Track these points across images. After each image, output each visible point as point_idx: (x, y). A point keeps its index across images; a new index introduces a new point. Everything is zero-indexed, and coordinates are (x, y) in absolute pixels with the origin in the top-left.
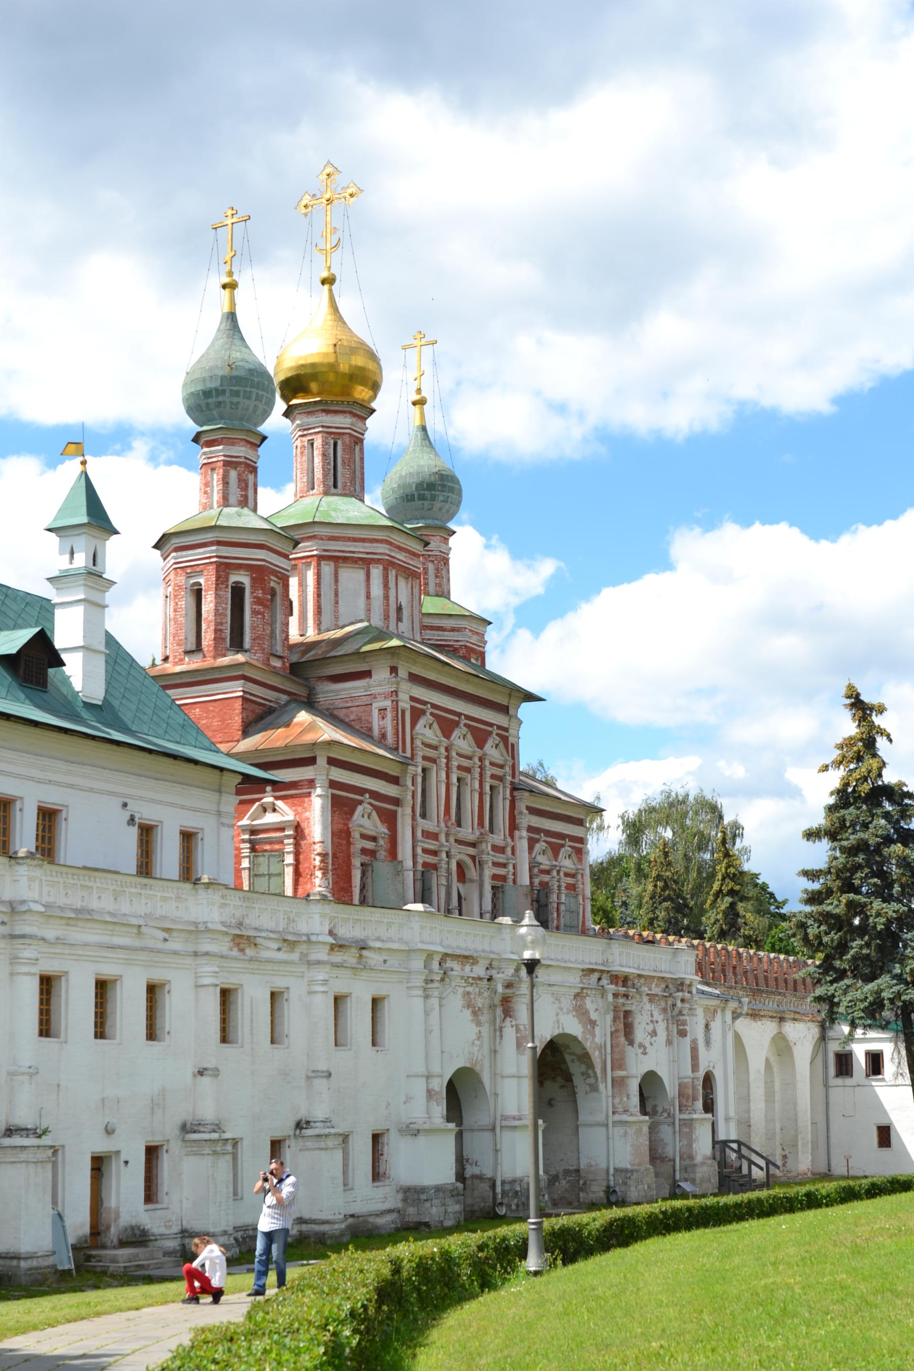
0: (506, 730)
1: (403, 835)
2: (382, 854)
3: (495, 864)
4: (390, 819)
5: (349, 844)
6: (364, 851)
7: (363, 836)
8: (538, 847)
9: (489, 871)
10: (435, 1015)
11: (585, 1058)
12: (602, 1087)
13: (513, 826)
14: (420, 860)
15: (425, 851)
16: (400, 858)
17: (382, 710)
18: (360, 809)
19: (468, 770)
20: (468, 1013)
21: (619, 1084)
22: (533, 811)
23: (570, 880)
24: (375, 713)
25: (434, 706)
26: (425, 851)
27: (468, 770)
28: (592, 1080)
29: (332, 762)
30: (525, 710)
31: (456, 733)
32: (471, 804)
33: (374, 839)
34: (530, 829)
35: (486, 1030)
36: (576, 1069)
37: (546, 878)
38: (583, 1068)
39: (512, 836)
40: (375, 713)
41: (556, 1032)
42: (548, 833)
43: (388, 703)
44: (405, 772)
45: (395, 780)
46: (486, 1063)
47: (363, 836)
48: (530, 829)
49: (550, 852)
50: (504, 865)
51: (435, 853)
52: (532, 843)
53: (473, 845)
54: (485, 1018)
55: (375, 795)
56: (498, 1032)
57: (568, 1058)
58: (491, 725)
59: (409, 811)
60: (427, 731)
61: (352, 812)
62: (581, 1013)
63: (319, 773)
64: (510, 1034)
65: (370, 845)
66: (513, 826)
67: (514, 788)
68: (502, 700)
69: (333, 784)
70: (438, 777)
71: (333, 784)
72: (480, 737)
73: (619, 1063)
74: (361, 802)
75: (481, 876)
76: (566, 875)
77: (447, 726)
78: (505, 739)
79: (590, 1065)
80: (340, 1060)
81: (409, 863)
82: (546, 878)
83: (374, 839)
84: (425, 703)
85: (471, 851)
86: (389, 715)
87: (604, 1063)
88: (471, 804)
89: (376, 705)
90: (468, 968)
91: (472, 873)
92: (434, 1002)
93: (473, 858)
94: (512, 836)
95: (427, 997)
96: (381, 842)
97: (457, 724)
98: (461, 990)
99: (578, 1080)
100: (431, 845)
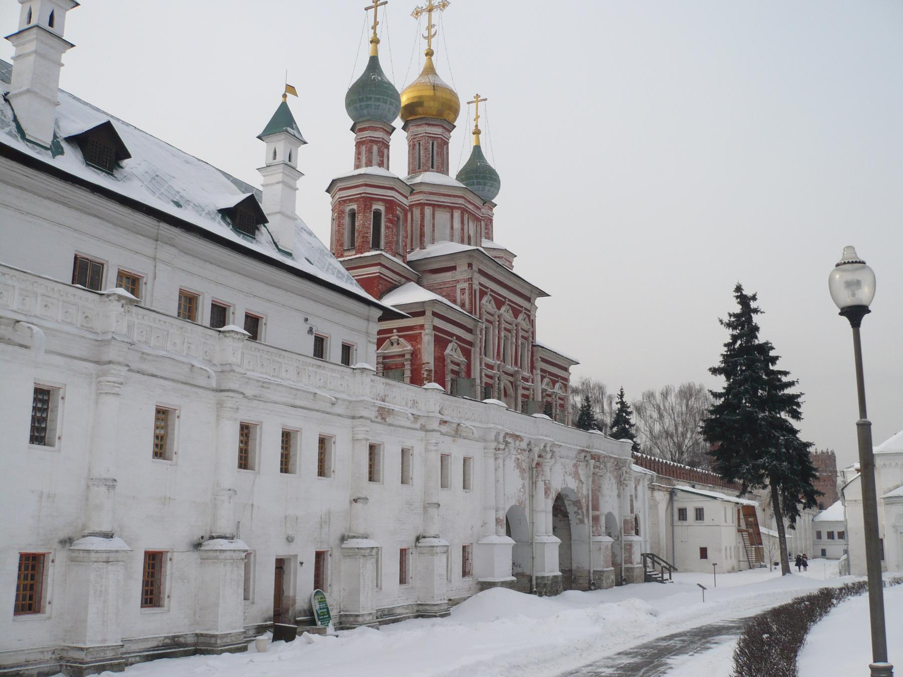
0: (529, 311)
1: (475, 364)
2: (463, 374)
3: (524, 388)
4: (467, 353)
5: (444, 366)
6: (453, 371)
7: (453, 362)
8: (546, 380)
9: (521, 391)
10: (501, 470)
11: (577, 503)
12: (586, 521)
13: (533, 367)
14: (484, 381)
15: (487, 376)
16: (472, 377)
17: (463, 290)
18: (450, 346)
19: (509, 331)
20: (517, 472)
21: (596, 519)
22: (544, 360)
23: (561, 402)
24: (458, 292)
25: (492, 291)
26: (487, 376)
27: (509, 331)
28: (580, 517)
29: (435, 314)
30: (539, 301)
31: (503, 309)
32: (511, 352)
33: (458, 365)
34: (542, 370)
35: (527, 482)
36: (571, 509)
37: (549, 399)
38: (575, 509)
39: (532, 372)
40: (458, 292)
41: (564, 486)
42: (551, 374)
43: (466, 285)
44: (476, 326)
45: (470, 331)
46: (527, 502)
47: (453, 362)
48: (542, 370)
49: (551, 384)
50: (528, 389)
51: (491, 377)
52: (543, 377)
53: (512, 375)
54: (527, 475)
55: (459, 338)
56: (533, 484)
57: (566, 502)
58: (522, 307)
59: (478, 350)
60: (487, 304)
61: (445, 347)
62: (576, 475)
63: (427, 321)
64: (541, 485)
65: (456, 368)
66: (533, 367)
67: (533, 346)
68: (527, 293)
69: (435, 328)
70: (493, 332)
71: (435, 328)
72: (516, 313)
73: (596, 508)
74: (451, 341)
75: (516, 393)
76: (560, 398)
77: (499, 304)
78: (529, 316)
79: (580, 508)
80: (442, 496)
81: (478, 381)
82: (549, 399)
83: (458, 365)
84: (487, 288)
85: (511, 379)
86: (467, 292)
87: (588, 506)
88: (511, 352)
89: (460, 286)
90: (517, 443)
91: (511, 391)
92: (500, 461)
93: (511, 383)
94: (532, 372)
95: (496, 459)
96: (463, 367)
97: (504, 303)
98: (514, 457)
99: (572, 516)
100: (490, 372)
